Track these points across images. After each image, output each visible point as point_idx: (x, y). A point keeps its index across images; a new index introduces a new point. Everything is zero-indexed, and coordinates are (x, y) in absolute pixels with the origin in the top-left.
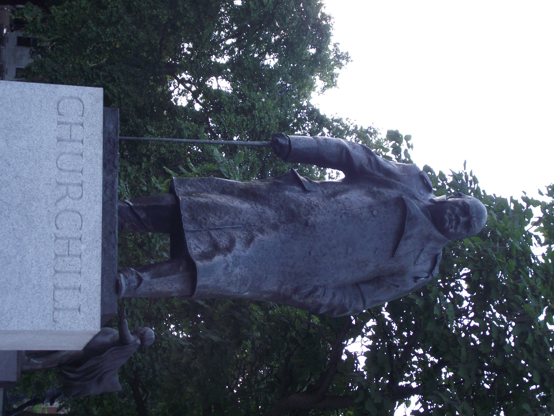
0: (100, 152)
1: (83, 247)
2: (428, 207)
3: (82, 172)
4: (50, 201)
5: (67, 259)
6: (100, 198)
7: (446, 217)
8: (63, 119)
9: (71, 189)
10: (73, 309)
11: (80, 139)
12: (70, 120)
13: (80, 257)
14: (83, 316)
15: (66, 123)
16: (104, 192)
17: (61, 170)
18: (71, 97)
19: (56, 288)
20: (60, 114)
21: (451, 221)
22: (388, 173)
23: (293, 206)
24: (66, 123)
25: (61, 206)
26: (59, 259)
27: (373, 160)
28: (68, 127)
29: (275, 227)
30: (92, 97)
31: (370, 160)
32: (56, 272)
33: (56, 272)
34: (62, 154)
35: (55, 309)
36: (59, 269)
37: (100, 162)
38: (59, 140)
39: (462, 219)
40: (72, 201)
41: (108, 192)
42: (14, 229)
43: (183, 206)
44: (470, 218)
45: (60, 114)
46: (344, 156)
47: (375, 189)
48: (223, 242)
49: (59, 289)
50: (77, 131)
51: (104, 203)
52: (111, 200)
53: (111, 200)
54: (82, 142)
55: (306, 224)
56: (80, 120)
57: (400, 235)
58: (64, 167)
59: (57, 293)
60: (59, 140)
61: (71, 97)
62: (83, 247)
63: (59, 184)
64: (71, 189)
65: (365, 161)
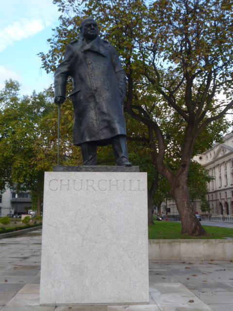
0: (73, 173)
1: (113, 179)
2: (87, 41)
3: (82, 180)
4: (95, 193)
5: (119, 186)
6: (93, 173)
7: (92, 34)
8: (59, 188)
9: (89, 184)
10: (139, 183)
11: (67, 181)
12: (59, 185)
13: (117, 181)
14: (141, 179)
15: (61, 187)
16: (90, 171)
17: (81, 189)
18: (49, 185)
19: (130, 190)
20: (57, 189)
21: (93, 32)
22: (71, 57)
23: (88, 96)
24: (61, 187)
25: (97, 188)
26: (119, 189)
27: (66, 63)
28: (62, 186)
29: (97, 103)
30: (146, 173)
31: (65, 64)
32: (124, 190)
33: (124, 190)
34: (74, 189)
35: (139, 189)
36: (122, 189)
37: (77, 173)
38: (68, 189)
39: (93, 27)
40: (94, 184)
41: (89, 170)
42: (107, 207)
43: (88, 140)
44: (92, 24)
45: (57, 189)
46: (61, 75)
47: (79, 62)
48: (105, 124)
49: (131, 188)
50: (65, 182)
51: (94, 171)
52: (93, 168)
53: (93, 168)
54: (69, 180)
55: (96, 90)
56: (59, 181)
57: (98, 53)
58: (80, 188)
59: (132, 189)
60: (68, 189)
61: (49, 185)
62: (113, 179)
63: (87, 189)
64: (89, 184)
65: (66, 66)
